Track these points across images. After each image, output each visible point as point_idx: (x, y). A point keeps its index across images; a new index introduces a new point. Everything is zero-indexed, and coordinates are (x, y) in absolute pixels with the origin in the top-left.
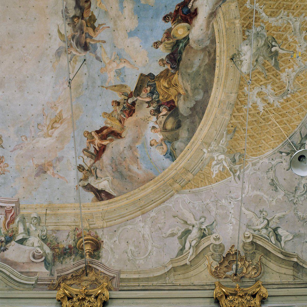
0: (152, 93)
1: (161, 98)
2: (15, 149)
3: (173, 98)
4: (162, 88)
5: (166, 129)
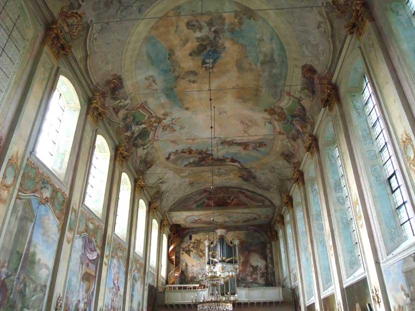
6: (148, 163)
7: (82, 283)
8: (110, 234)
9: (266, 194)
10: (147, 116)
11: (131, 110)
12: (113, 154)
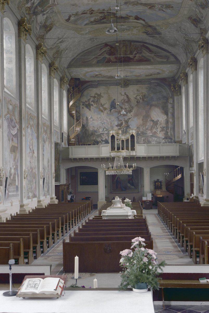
6: (47, 28)
7: (11, 154)
8: (24, 109)
9: (170, 49)
12: (17, 32)
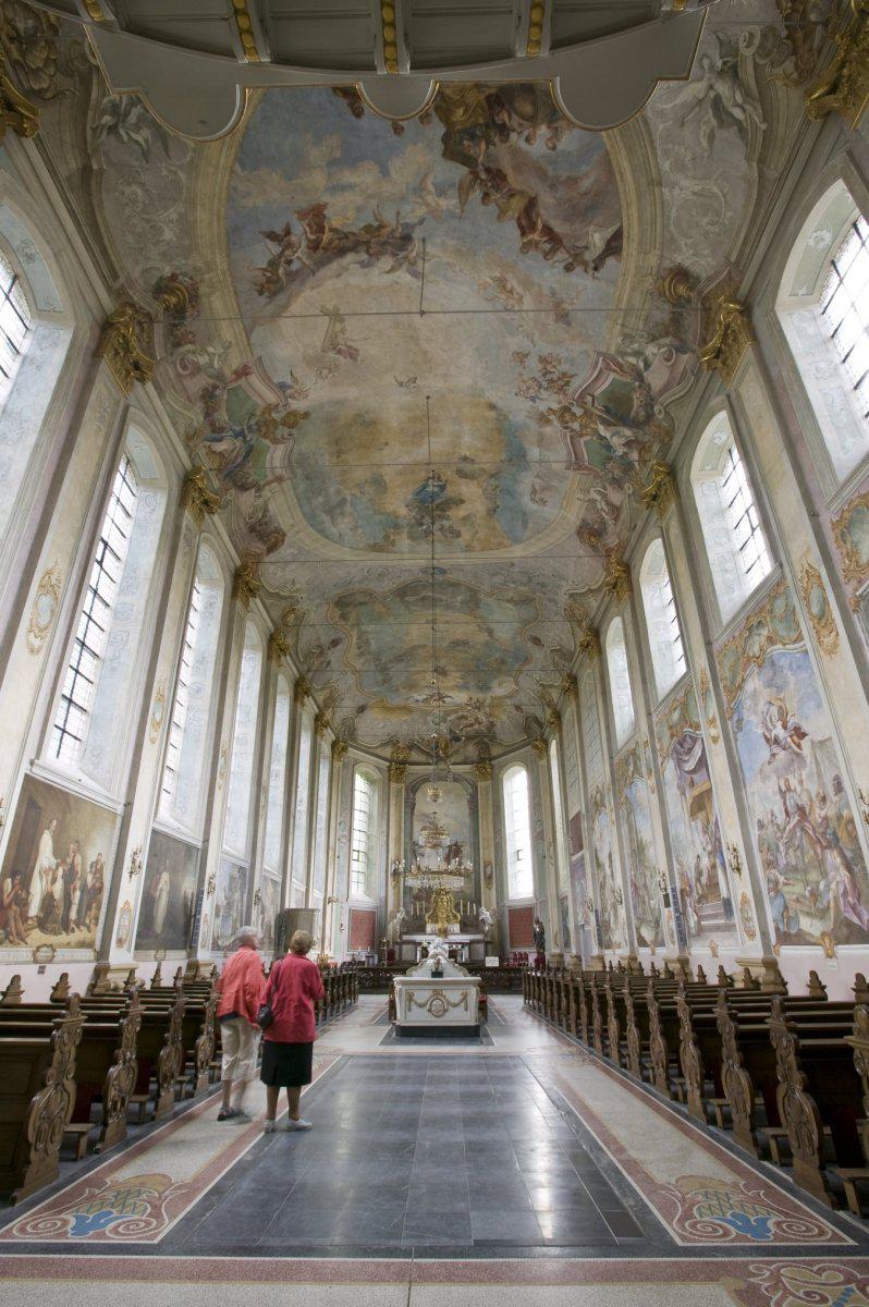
0: (472, 137)
1: (481, 121)
2: (533, 341)
3: (483, 97)
4: (464, 118)
5: (533, 117)
10: (582, 440)
11: (601, 478)
